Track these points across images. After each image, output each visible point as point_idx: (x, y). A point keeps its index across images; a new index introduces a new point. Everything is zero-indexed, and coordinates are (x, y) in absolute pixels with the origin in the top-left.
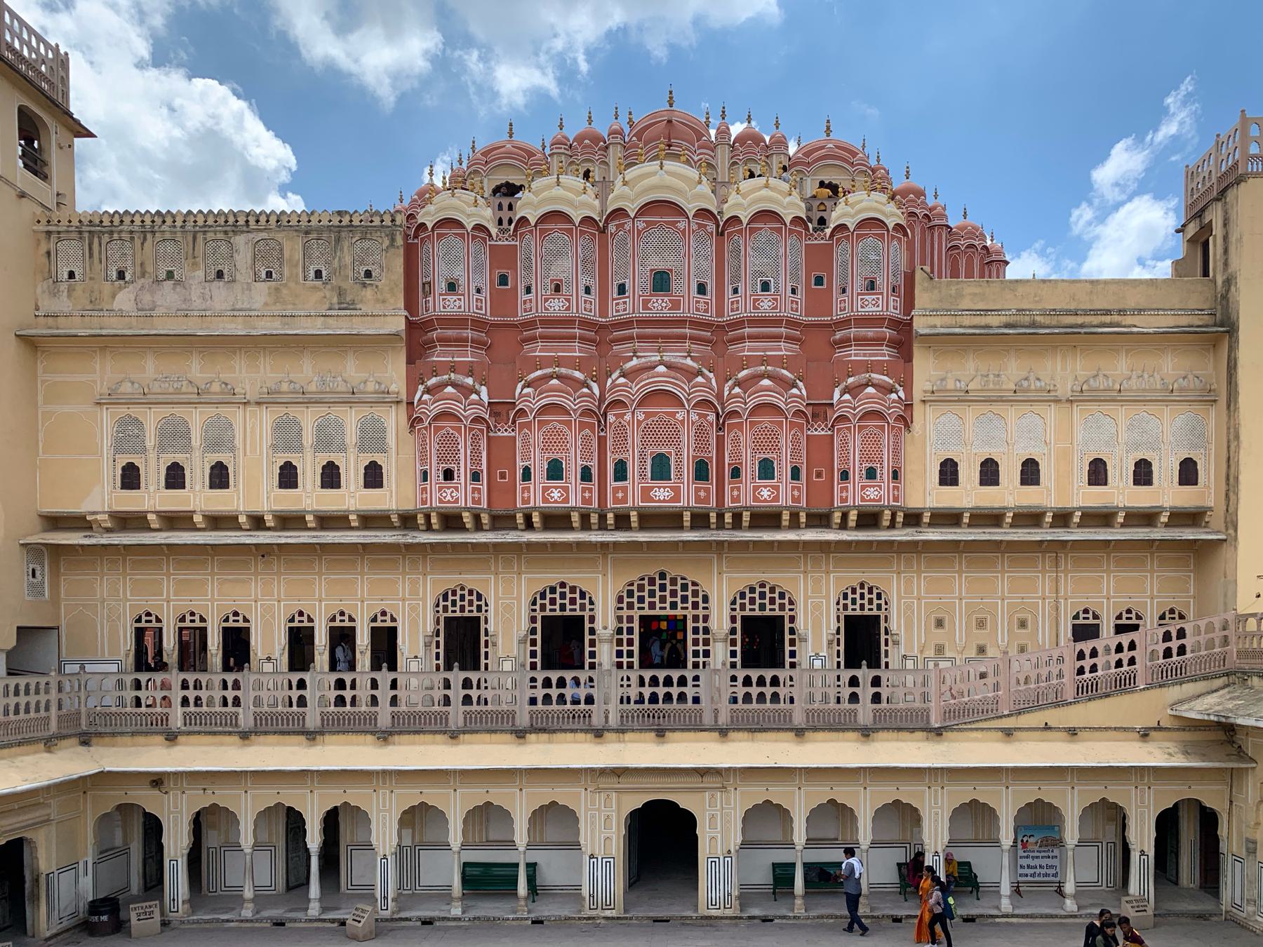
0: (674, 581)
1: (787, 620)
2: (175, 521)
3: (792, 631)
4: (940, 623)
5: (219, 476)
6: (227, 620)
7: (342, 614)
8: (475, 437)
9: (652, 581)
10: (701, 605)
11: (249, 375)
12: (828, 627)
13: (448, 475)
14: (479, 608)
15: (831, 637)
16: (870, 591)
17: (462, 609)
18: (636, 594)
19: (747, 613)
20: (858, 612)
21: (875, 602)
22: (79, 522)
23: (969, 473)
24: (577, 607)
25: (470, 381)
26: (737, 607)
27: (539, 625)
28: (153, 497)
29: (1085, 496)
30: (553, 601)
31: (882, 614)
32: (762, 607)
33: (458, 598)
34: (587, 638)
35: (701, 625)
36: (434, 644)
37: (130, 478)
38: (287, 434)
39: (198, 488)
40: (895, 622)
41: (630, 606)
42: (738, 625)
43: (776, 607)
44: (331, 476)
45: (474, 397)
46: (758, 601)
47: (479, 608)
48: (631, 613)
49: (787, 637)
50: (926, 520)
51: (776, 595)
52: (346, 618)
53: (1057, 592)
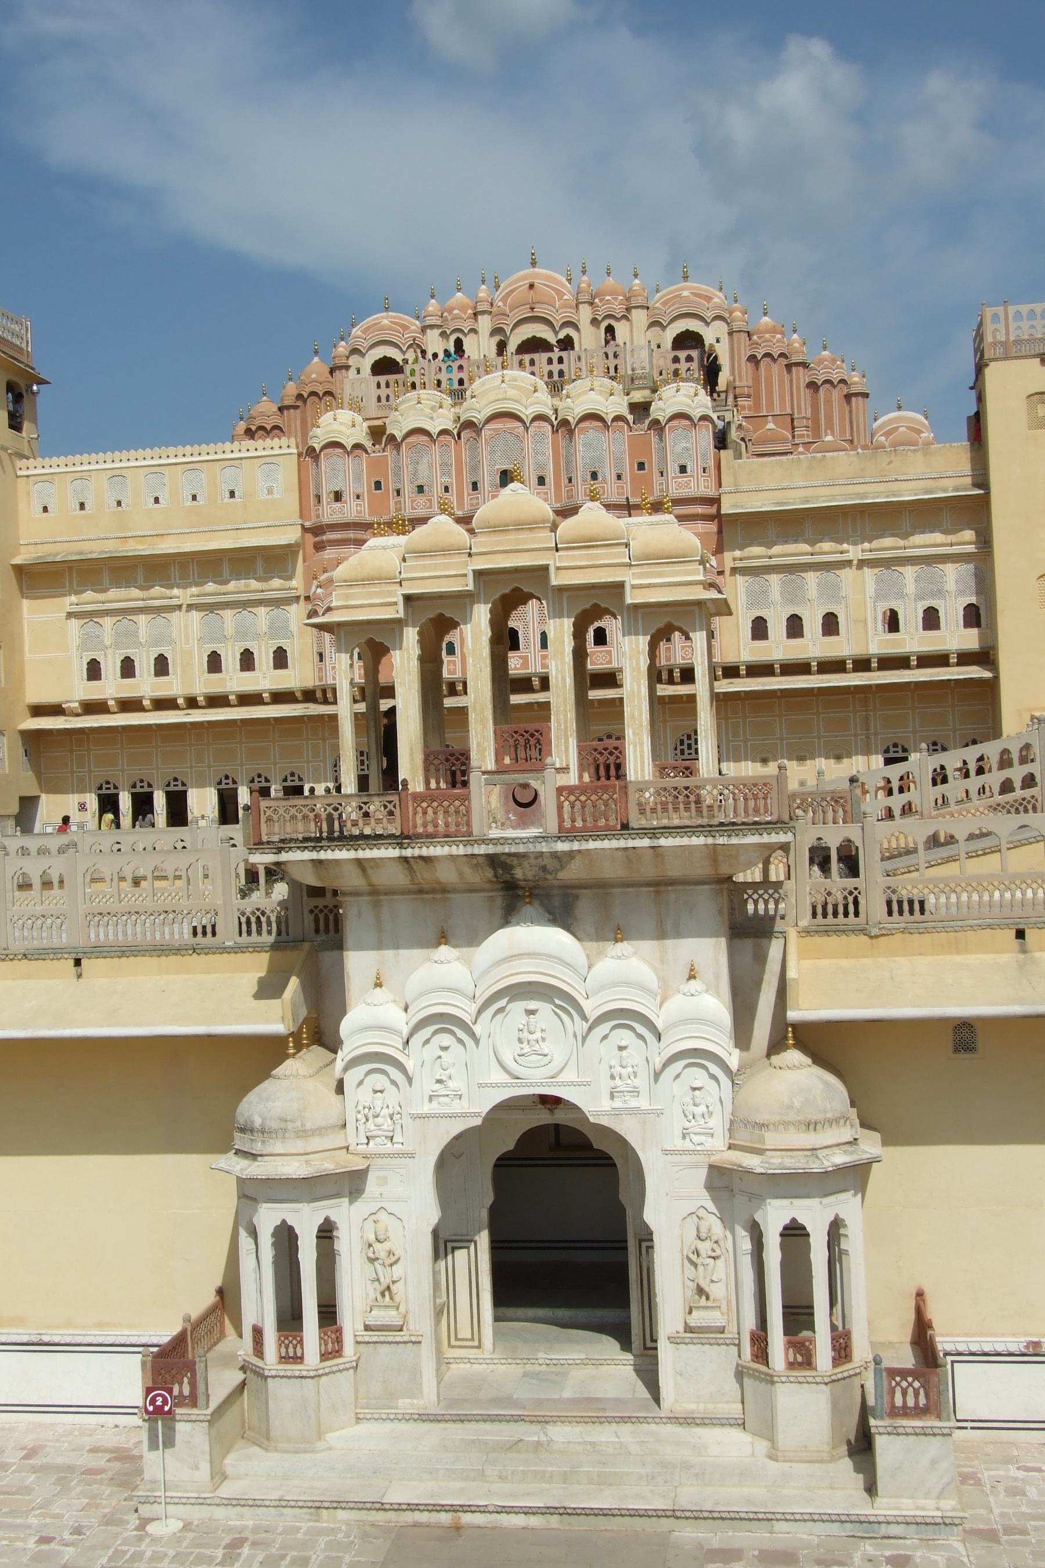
5: (162, 666)
6: (168, 785)
7: (259, 776)
22: (56, 710)
23: (777, 628)
28: (111, 687)
29: (878, 643)
37: (94, 671)
39: (145, 675)
44: (247, 661)
53: (868, 729)
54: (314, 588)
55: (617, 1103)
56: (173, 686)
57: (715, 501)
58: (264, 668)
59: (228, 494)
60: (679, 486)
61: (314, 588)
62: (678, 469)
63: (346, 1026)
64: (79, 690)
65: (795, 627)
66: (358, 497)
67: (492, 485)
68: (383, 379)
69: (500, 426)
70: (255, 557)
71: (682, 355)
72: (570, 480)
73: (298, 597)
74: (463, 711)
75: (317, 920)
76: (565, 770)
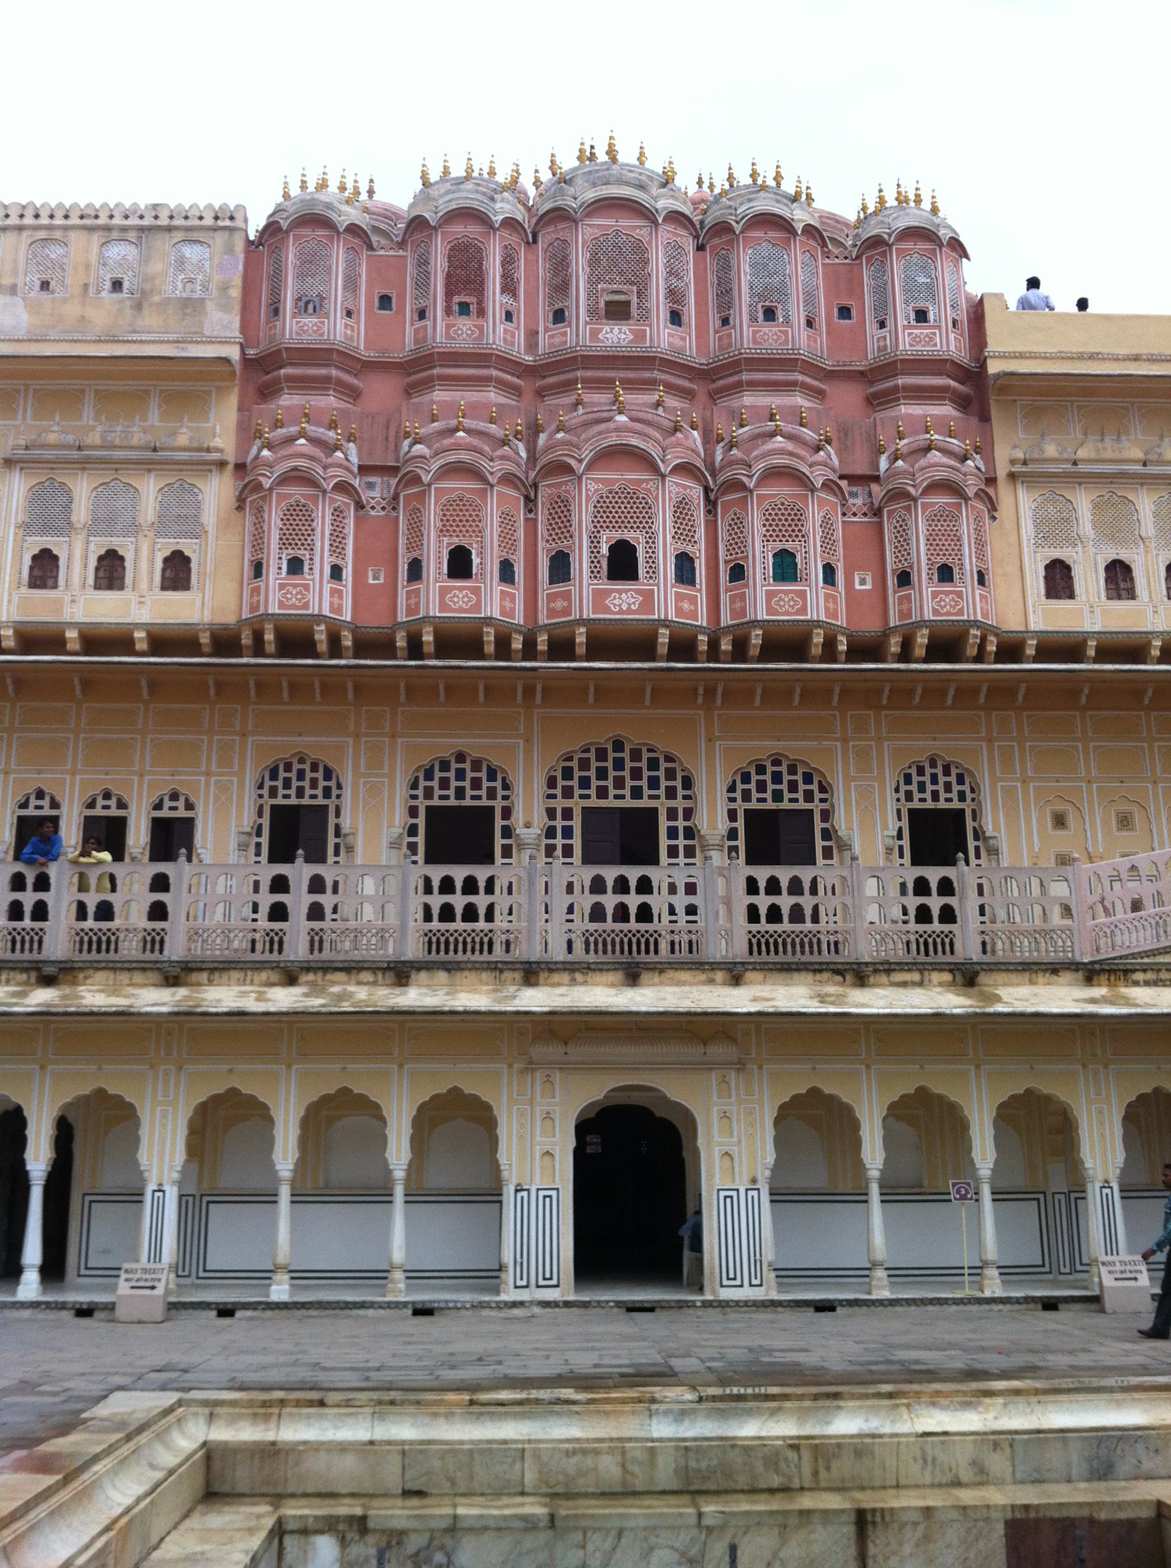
0: (636, 755)
1: (817, 817)
3: (826, 835)
4: (1060, 821)
8: (338, 513)
9: (601, 755)
10: (680, 792)
12: (885, 827)
13: (295, 566)
14: (327, 793)
15: (890, 842)
16: (947, 772)
17: (300, 793)
18: (577, 774)
19: (754, 805)
20: (929, 805)
21: (956, 788)
23: (1089, 580)
24: (483, 793)
25: (331, 434)
26: (738, 795)
27: (421, 821)
30: (444, 784)
31: (968, 806)
32: (778, 796)
33: (293, 775)
34: (499, 842)
35: (680, 824)
36: (252, 849)
38: (48, 513)
41: (568, 793)
42: (740, 825)
43: (800, 796)
44: (110, 573)
45: (339, 454)
46: (771, 787)
47: (327, 793)
48: (568, 803)
49: (819, 844)
50: (1030, 652)
51: (799, 778)
52: (113, 803)
54: (254, 451)
58: (143, 585)
59: (108, 285)
60: (915, 340)
61: (254, 451)
62: (912, 315)
66: (349, 314)
67: (592, 312)
69: (611, 222)
70: (147, 392)
72: (725, 321)
73: (222, 464)
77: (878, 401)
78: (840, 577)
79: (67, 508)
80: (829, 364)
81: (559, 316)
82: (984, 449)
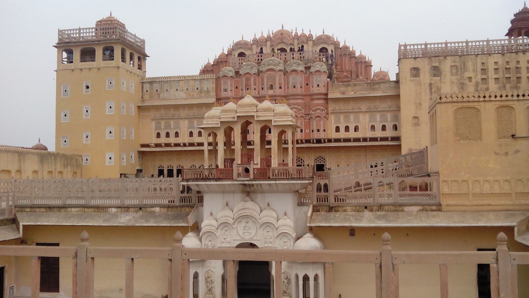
2: (168, 145)
4: (338, 166)
5: (177, 135)
11: (183, 113)
22: (148, 146)
23: (342, 129)
28: (163, 140)
29: (369, 134)
38: (191, 126)
40: (328, 166)
55: (266, 245)
56: (179, 140)
57: (327, 94)
63: (203, 225)
64: (155, 140)
65: (347, 129)
68: (241, 58)
71: (322, 54)
74: (253, 150)
75: (199, 199)
76: (257, 164)
77: (312, 99)
78: (303, 131)
79: (193, 125)
80: (304, 94)
81: (262, 89)
82: (327, 108)
